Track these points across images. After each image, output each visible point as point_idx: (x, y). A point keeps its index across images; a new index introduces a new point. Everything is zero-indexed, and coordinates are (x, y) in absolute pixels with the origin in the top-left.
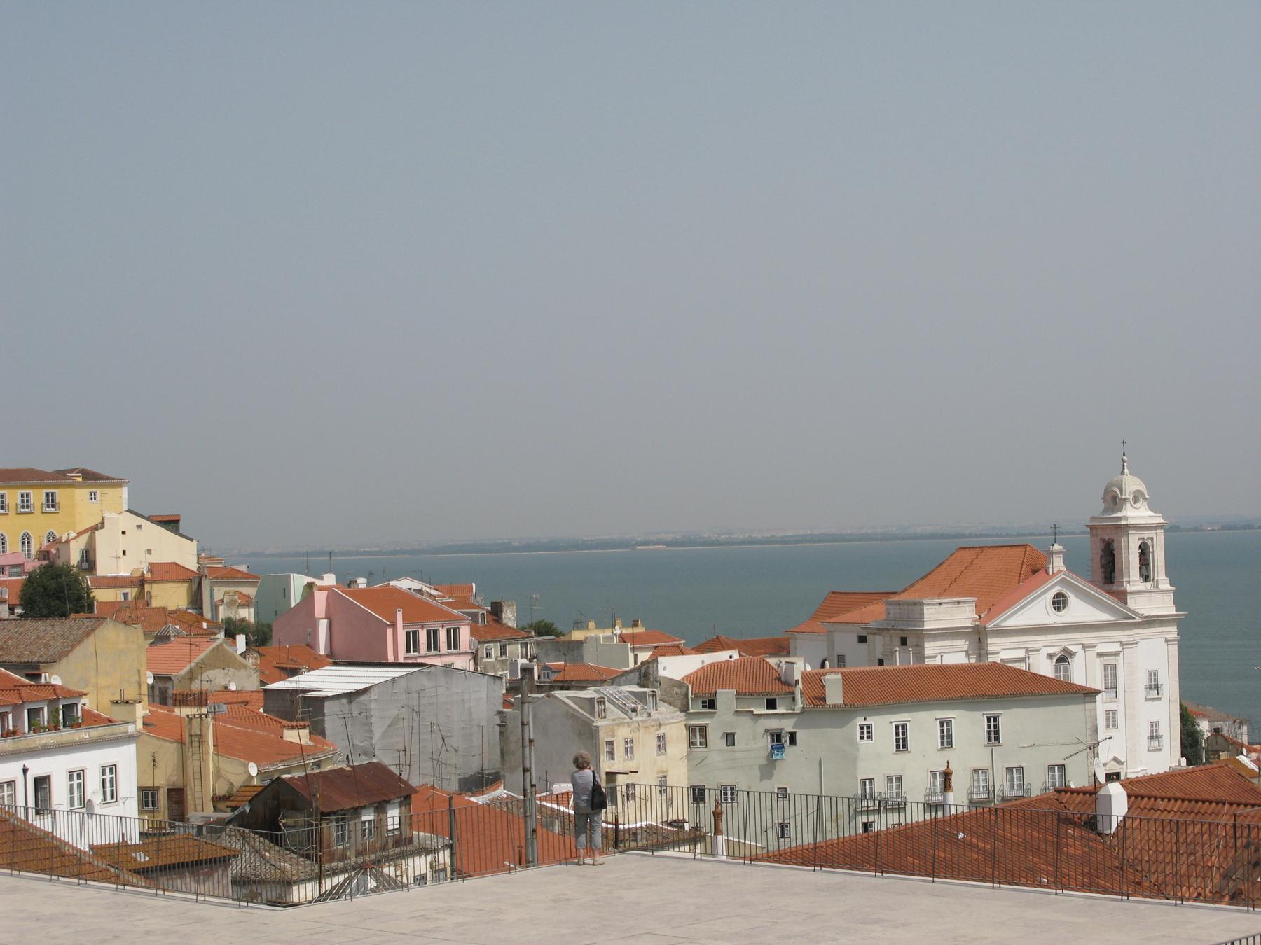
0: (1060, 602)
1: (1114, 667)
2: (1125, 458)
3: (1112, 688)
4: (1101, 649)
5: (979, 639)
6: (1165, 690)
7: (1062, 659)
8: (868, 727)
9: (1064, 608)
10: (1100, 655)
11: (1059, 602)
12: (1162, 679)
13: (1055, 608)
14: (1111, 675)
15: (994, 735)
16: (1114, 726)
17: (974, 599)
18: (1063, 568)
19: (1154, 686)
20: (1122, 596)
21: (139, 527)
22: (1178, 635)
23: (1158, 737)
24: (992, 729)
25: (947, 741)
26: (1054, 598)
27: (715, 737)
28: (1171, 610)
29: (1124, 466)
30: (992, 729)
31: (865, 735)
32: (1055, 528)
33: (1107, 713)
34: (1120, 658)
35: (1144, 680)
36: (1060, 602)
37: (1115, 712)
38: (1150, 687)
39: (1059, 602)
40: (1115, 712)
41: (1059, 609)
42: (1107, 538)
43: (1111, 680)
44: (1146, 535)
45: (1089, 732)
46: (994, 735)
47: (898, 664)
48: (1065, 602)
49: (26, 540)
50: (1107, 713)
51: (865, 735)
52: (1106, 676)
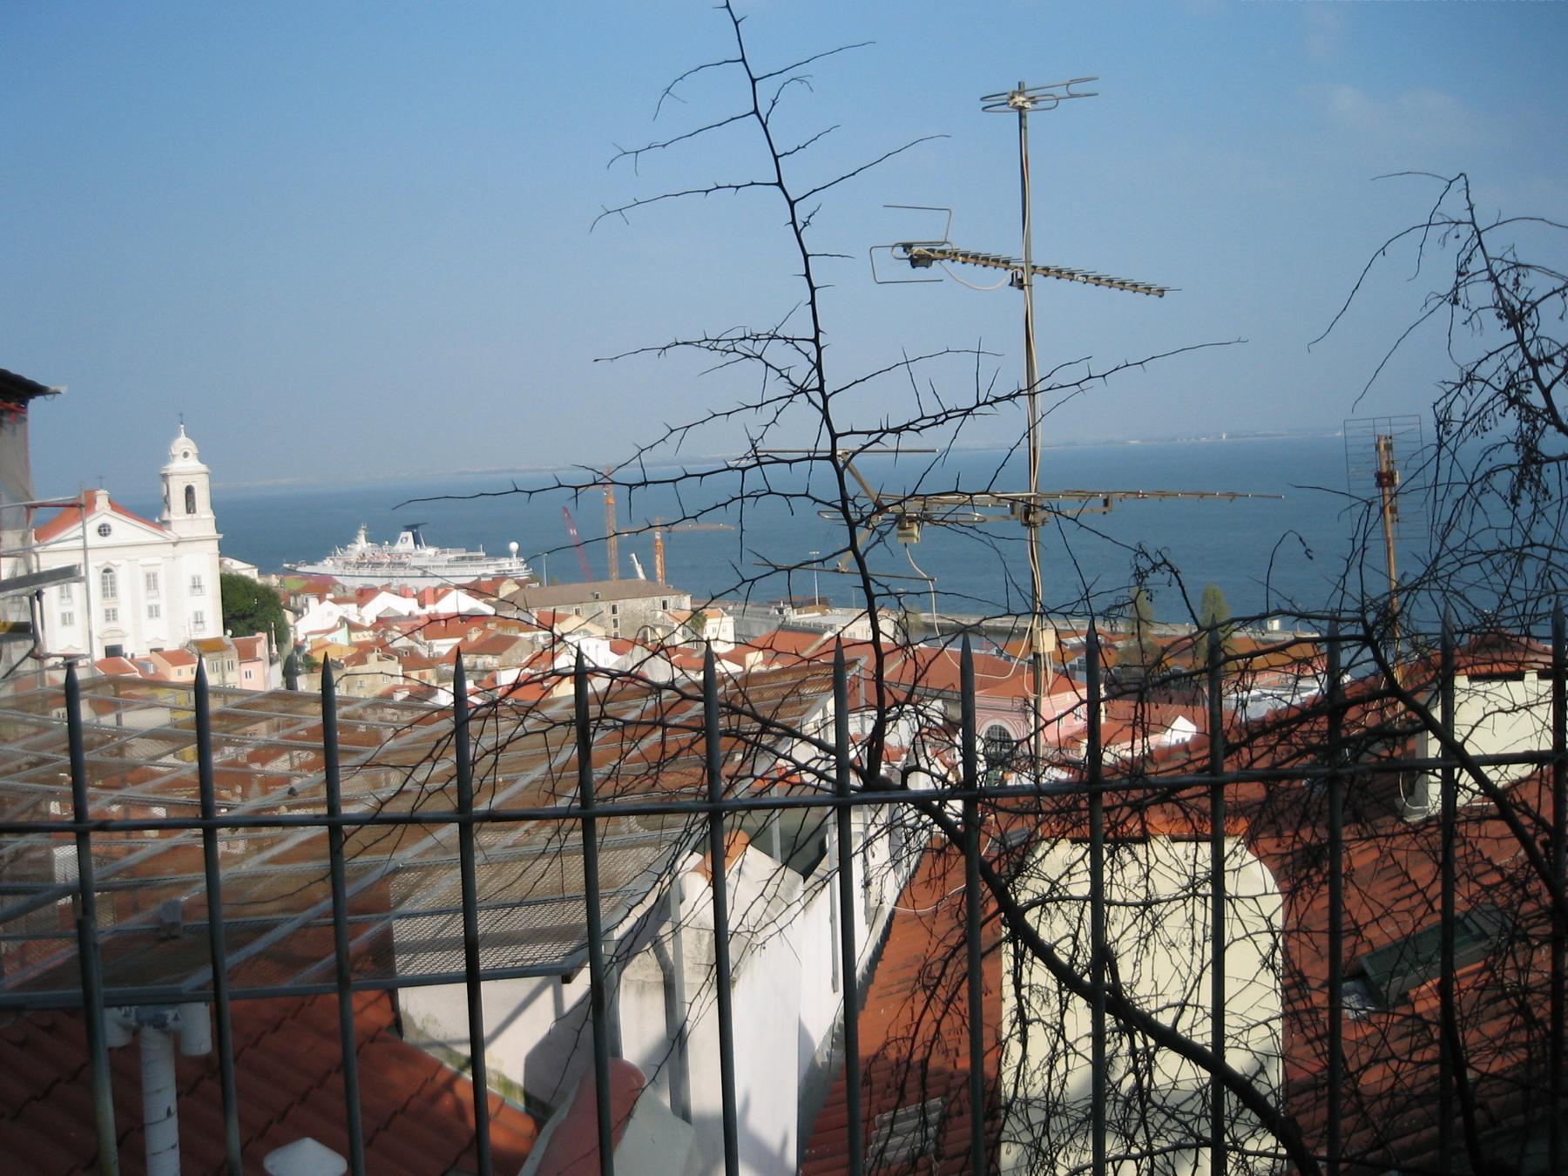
1: (155, 575)
4: (142, 562)
7: (107, 571)
10: (143, 566)
19: (196, 585)
20: (164, 525)
28: (213, 533)
36: (104, 530)
38: (195, 587)
41: (105, 535)
44: (189, 481)
52: (148, 581)
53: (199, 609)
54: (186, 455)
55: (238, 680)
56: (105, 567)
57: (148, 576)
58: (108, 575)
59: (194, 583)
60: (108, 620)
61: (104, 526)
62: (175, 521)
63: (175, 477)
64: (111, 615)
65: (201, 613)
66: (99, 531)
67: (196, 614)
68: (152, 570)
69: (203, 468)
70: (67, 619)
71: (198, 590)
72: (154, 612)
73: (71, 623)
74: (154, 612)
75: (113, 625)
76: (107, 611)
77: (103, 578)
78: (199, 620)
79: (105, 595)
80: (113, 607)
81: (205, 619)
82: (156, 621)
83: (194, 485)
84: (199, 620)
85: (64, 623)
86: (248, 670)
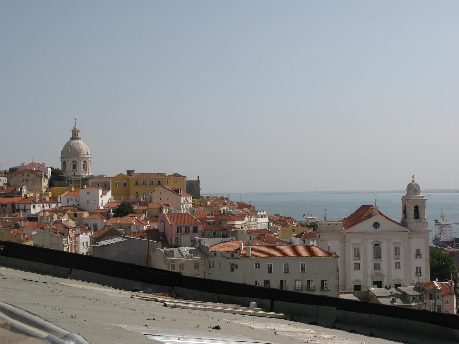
0: (376, 225)
3: (398, 255)
6: (423, 256)
7: (377, 245)
8: (258, 265)
9: (378, 227)
11: (376, 225)
12: (422, 252)
14: (398, 250)
15: (303, 270)
19: (418, 254)
21: (165, 192)
23: (420, 272)
25: (286, 271)
26: (374, 223)
27: (216, 265)
31: (257, 267)
32: (376, 200)
33: (396, 263)
34: (402, 244)
35: (414, 252)
37: (399, 263)
38: (417, 255)
39: (376, 225)
40: (399, 263)
41: (376, 228)
42: (405, 204)
46: (303, 270)
48: (379, 225)
49: (144, 194)
50: (396, 263)
51: (257, 267)
52: (396, 251)
53: (418, 266)
55: (441, 304)
57: (396, 248)
58: (377, 247)
59: (417, 253)
60: (375, 268)
61: (376, 223)
64: (377, 266)
66: (374, 225)
68: (397, 245)
70: (357, 267)
72: (398, 266)
74: (398, 266)
75: (378, 271)
76: (375, 264)
77: (374, 248)
78: (419, 272)
79: (375, 257)
81: (422, 270)
82: (399, 270)
83: (419, 205)
84: (419, 272)
85: (355, 269)
86: (447, 299)
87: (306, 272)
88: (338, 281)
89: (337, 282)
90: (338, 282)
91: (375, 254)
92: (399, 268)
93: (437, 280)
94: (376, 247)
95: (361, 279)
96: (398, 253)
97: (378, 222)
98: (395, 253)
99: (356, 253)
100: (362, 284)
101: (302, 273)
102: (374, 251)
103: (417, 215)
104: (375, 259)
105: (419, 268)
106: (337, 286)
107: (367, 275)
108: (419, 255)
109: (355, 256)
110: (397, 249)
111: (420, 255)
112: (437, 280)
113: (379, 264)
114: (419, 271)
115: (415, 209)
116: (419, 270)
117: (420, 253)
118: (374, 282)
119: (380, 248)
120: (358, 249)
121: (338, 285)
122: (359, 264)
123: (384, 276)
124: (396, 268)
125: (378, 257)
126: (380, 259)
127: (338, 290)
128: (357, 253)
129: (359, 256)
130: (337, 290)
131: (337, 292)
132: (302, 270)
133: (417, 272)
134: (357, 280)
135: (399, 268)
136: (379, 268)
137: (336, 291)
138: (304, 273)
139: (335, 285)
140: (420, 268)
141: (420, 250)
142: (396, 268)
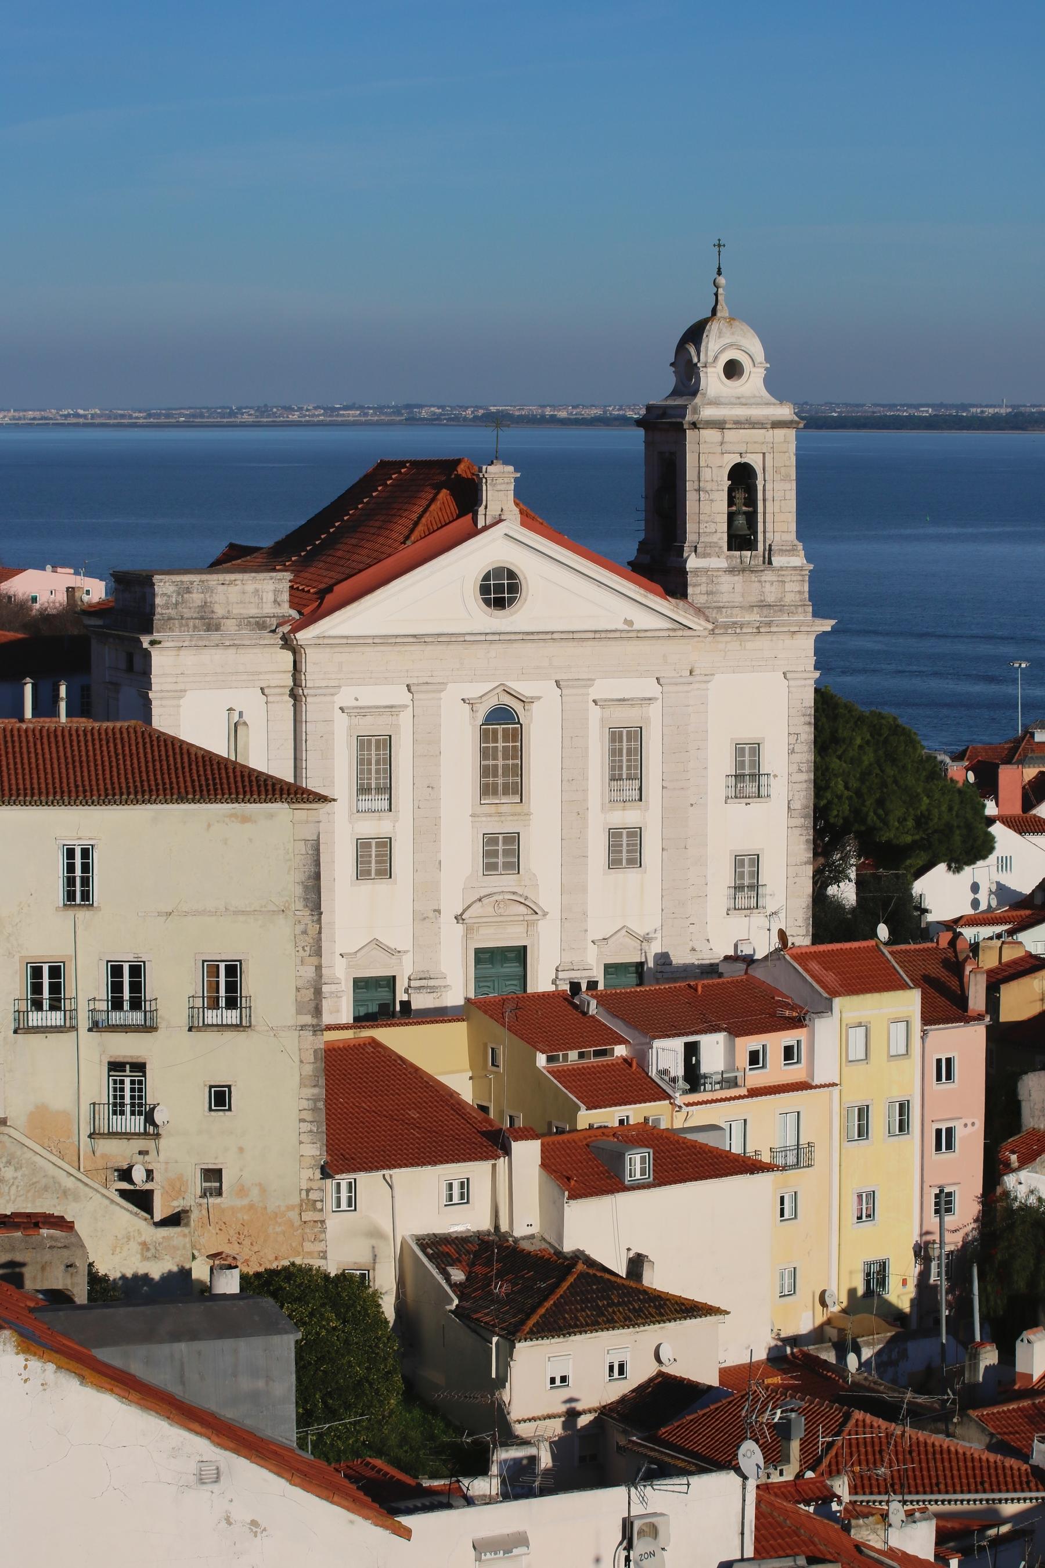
2: (722, 280)
3: (629, 778)
4: (603, 689)
5: (314, 664)
9: (512, 601)
11: (499, 588)
13: (487, 602)
16: (631, 862)
17: (288, 576)
18: (513, 513)
22: (816, 668)
23: (755, 887)
24: (78, 872)
26: (487, 577)
29: (716, 295)
30: (78, 872)
33: (614, 834)
34: (654, 711)
35: (721, 764)
38: (739, 777)
41: (499, 604)
43: (628, 761)
45: (299, 890)
47: (28, 713)
48: (514, 588)
54: (733, 370)
56: (492, 702)
57: (615, 736)
59: (739, 764)
60: (490, 867)
62: (697, 571)
63: (709, 435)
65: (756, 860)
66: (484, 589)
67: (739, 861)
68: (626, 717)
69: (785, 412)
71: (750, 788)
73: (386, 872)
76: (490, 840)
77: (486, 736)
79: (487, 790)
80: (509, 827)
82: (630, 876)
83: (754, 461)
85: (362, 873)
87: (99, 908)
88: (314, 960)
89: (309, 972)
90: (319, 968)
91: (486, 772)
92: (636, 861)
93: (883, 931)
94: (495, 731)
95: (399, 937)
96: (629, 768)
97: (512, 568)
98: (613, 768)
99: (369, 771)
100: (404, 971)
101: (70, 913)
102: (485, 754)
103: (741, 520)
104: (487, 809)
105: (751, 861)
106: (309, 994)
107: (438, 911)
108: (752, 781)
109: (363, 790)
110: (621, 741)
111: (755, 777)
112: (883, 931)
113: (513, 839)
114: (746, 882)
115: (731, 490)
116: (752, 874)
117: (756, 763)
118: (478, 952)
119: (517, 736)
120: (386, 743)
121: (318, 992)
122: (386, 844)
123: (545, 914)
124: (614, 863)
125: (506, 792)
126: (518, 808)
127: (315, 1022)
128: (378, 771)
129: (387, 789)
130: (308, 1019)
131: (308, 1034)
132: (70, 896)
133: (738, 888)
134: (377, 943)
135: (636, 861)
136: (514, 866)
137: (303, 1027)
138: (82, 915)
139: (298, 990)
140: (756, 860)
141: (756, 749)
142: (614, 863)
